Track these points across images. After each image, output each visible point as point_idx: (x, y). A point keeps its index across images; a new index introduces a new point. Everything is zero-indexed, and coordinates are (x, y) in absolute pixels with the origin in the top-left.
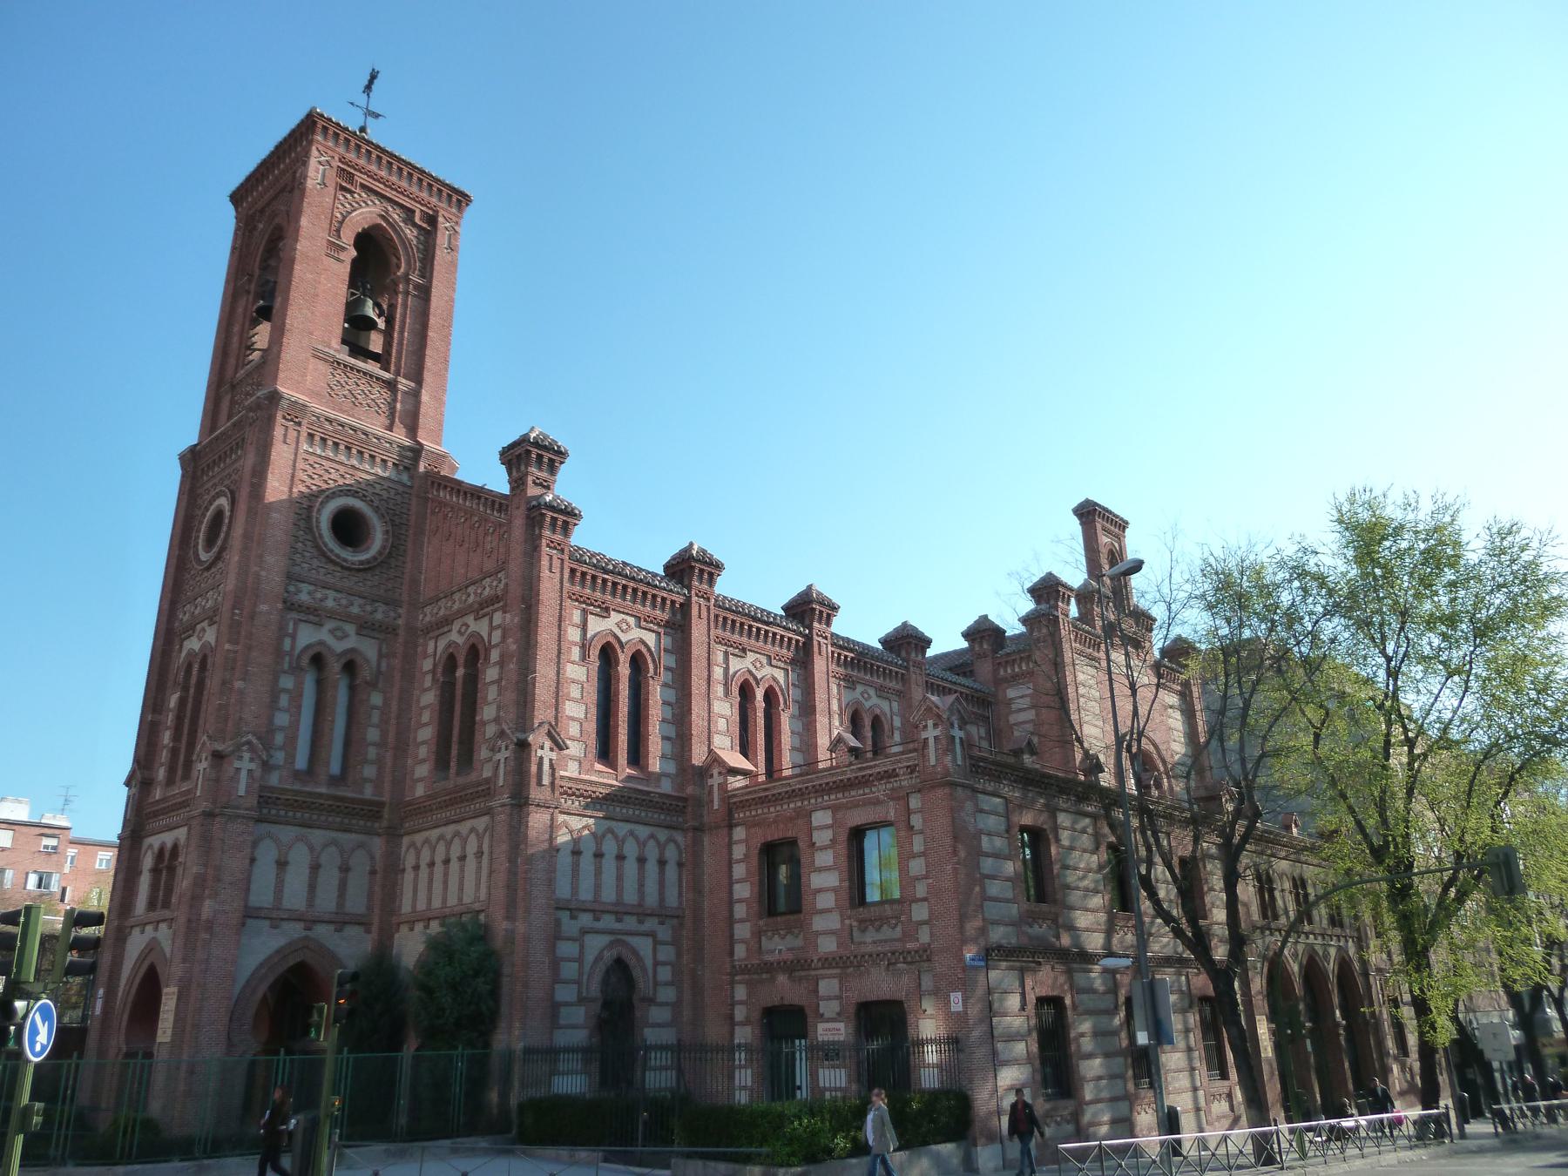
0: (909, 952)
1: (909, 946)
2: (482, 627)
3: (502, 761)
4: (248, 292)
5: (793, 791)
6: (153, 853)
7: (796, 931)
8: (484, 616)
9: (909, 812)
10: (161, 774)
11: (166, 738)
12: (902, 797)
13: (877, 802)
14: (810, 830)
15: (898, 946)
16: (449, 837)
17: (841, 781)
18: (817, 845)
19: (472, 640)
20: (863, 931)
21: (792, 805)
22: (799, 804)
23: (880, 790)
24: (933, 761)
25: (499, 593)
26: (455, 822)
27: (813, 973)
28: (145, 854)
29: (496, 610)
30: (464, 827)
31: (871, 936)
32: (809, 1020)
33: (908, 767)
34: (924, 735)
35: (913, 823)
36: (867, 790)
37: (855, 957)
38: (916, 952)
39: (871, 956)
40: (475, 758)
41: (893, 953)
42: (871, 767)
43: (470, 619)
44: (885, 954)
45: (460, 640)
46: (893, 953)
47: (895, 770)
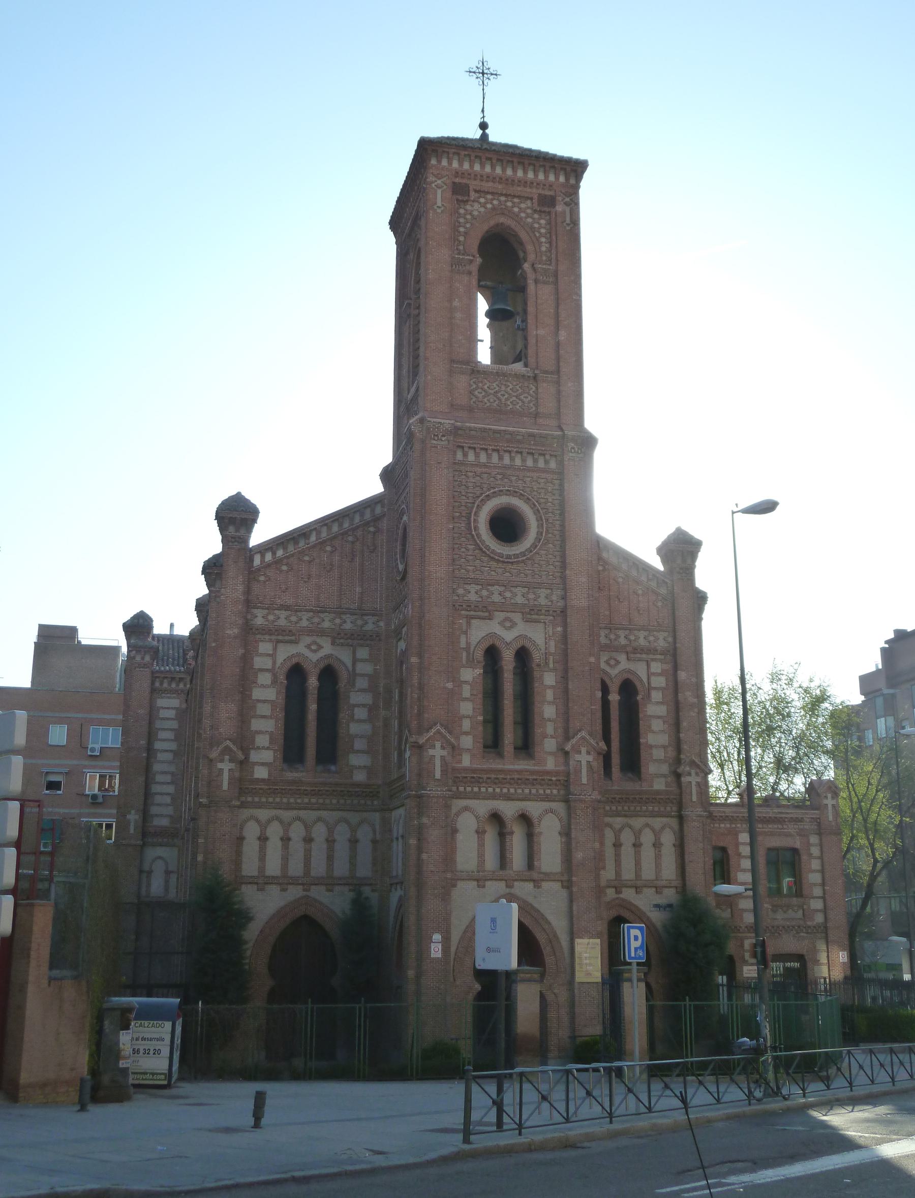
0: (809, 927)
1: (809, 923)
2: (640, 670)
3: (694, 783)
4: (470, 273)
5: (727, 816)
6: (477, 817)
7: (724, 907)
8: (640, 660)
9: (809, 844)
10: (467, 742)
11: (466, 708)
12: (803, 834)
13: (788, 835)
14: (737, 844)
15: (801, 922)
16: (618, 827)
17: (765, 817)
18: (743, 854)
19: (625, 676)
20: (774, 911)
21: (722, 825)
22: (728, 826)
23: (791, 828)
24: (831, 818)
25: (659, 648)
26: (626, 816)
27: (740, 935)
28: (458, 814)
29: (653, 660)
30: (638, 822)
31: (780, 915)
32: (737, 964)
33: (812, 818)
34: (825, 802)
35: (812, 852)
36: (780, 826)
37: (773, 927)
38: (814, 927)
39: (784, 927)
40: (643, 770)
41: (799, 927)
42: (787, 813)
43: (622, 658)
44: (793, 927)
45: (613, 672)
46: (799, 927)
47: (802, 818)
